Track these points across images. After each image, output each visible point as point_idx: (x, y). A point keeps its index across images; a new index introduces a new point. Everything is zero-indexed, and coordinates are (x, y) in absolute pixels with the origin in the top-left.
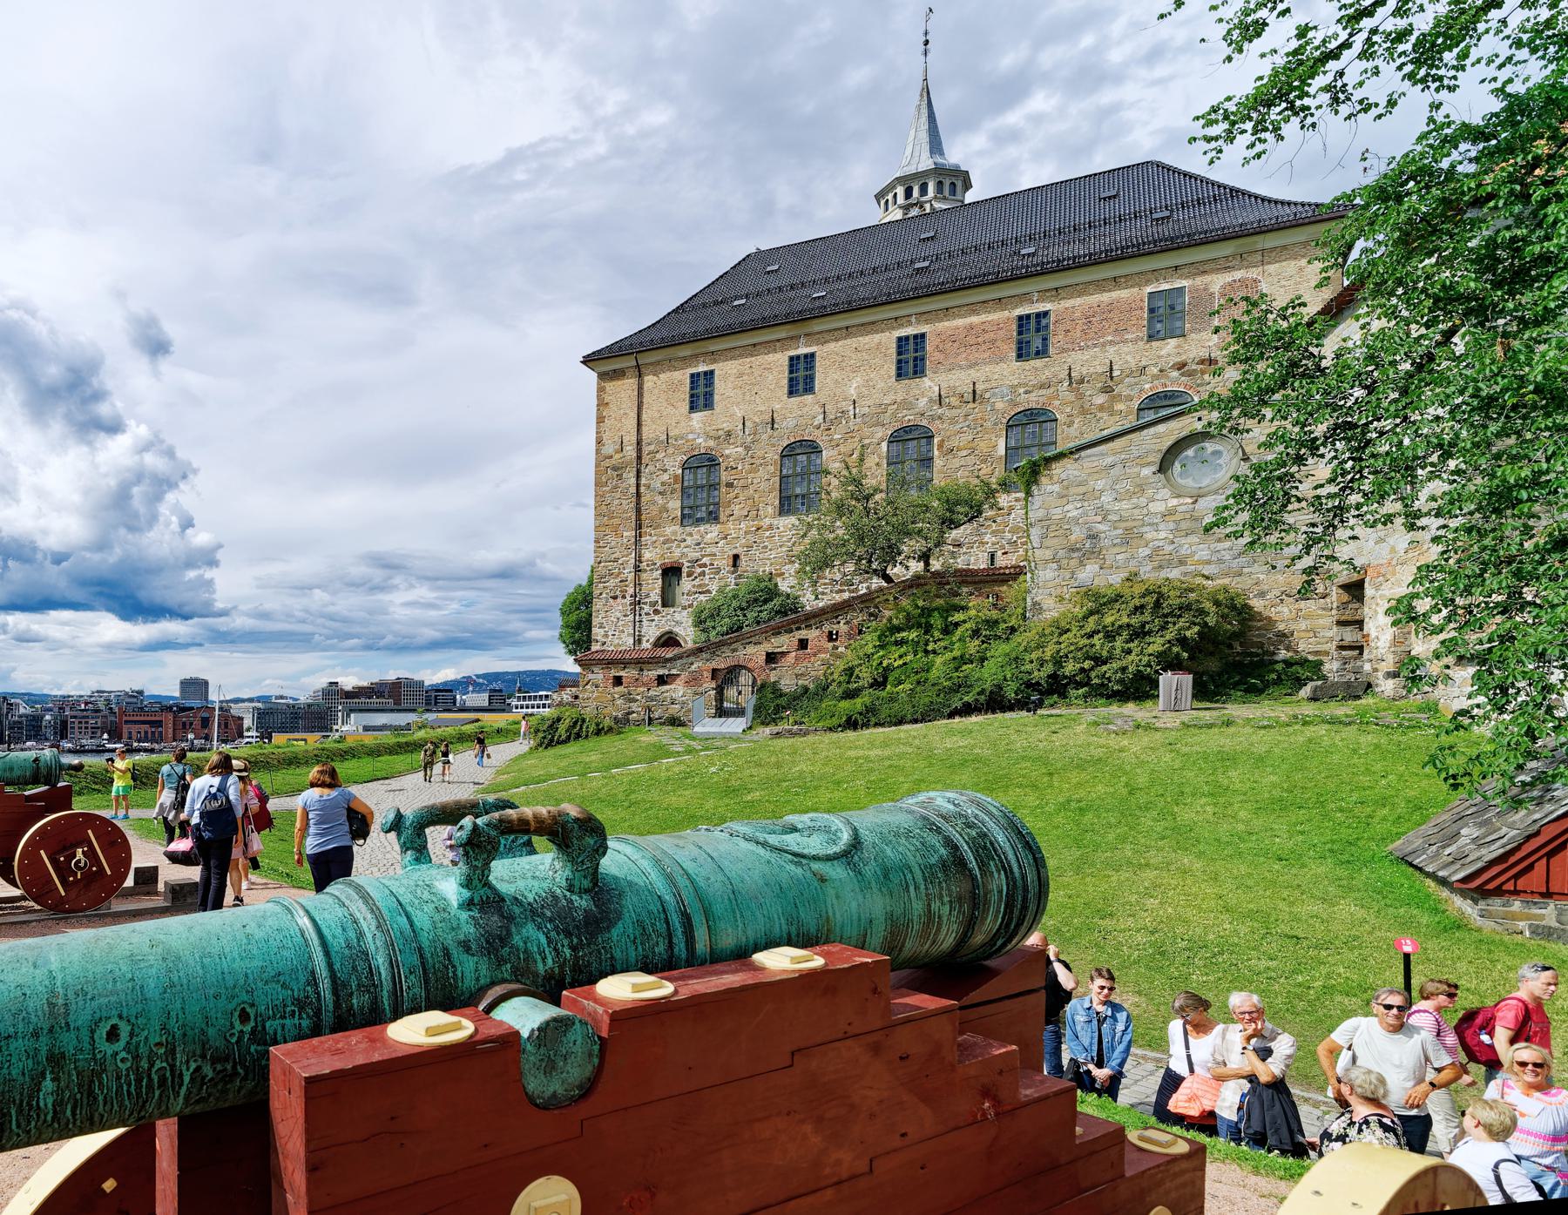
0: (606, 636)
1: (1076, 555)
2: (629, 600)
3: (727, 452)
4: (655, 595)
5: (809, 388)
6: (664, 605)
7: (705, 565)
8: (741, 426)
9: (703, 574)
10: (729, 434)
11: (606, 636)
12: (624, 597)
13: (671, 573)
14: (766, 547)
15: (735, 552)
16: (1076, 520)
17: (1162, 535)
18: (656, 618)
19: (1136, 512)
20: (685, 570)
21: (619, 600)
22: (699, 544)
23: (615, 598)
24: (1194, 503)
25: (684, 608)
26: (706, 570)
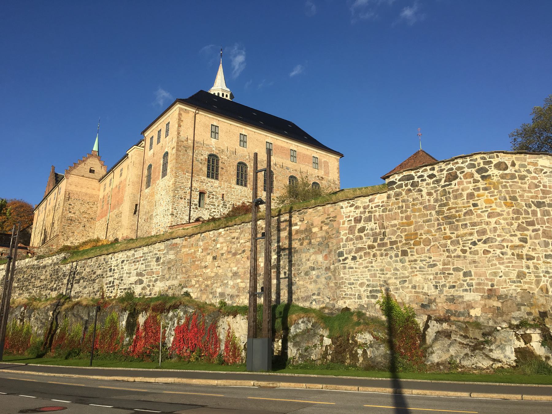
0: (177, 214)
4: (196, 201)
6: (199, 206)
7: (213, 195)
8: (226, 149)
9: (213, 198)
11: (177, 214)
12: (185, 199)
13: (202, 194)
14: (232, 194)
18: (196, 211)
21: (183, 199)
22: (212, 186)
23: (181, 198)
25: (206, 209)
26: (214, 197)
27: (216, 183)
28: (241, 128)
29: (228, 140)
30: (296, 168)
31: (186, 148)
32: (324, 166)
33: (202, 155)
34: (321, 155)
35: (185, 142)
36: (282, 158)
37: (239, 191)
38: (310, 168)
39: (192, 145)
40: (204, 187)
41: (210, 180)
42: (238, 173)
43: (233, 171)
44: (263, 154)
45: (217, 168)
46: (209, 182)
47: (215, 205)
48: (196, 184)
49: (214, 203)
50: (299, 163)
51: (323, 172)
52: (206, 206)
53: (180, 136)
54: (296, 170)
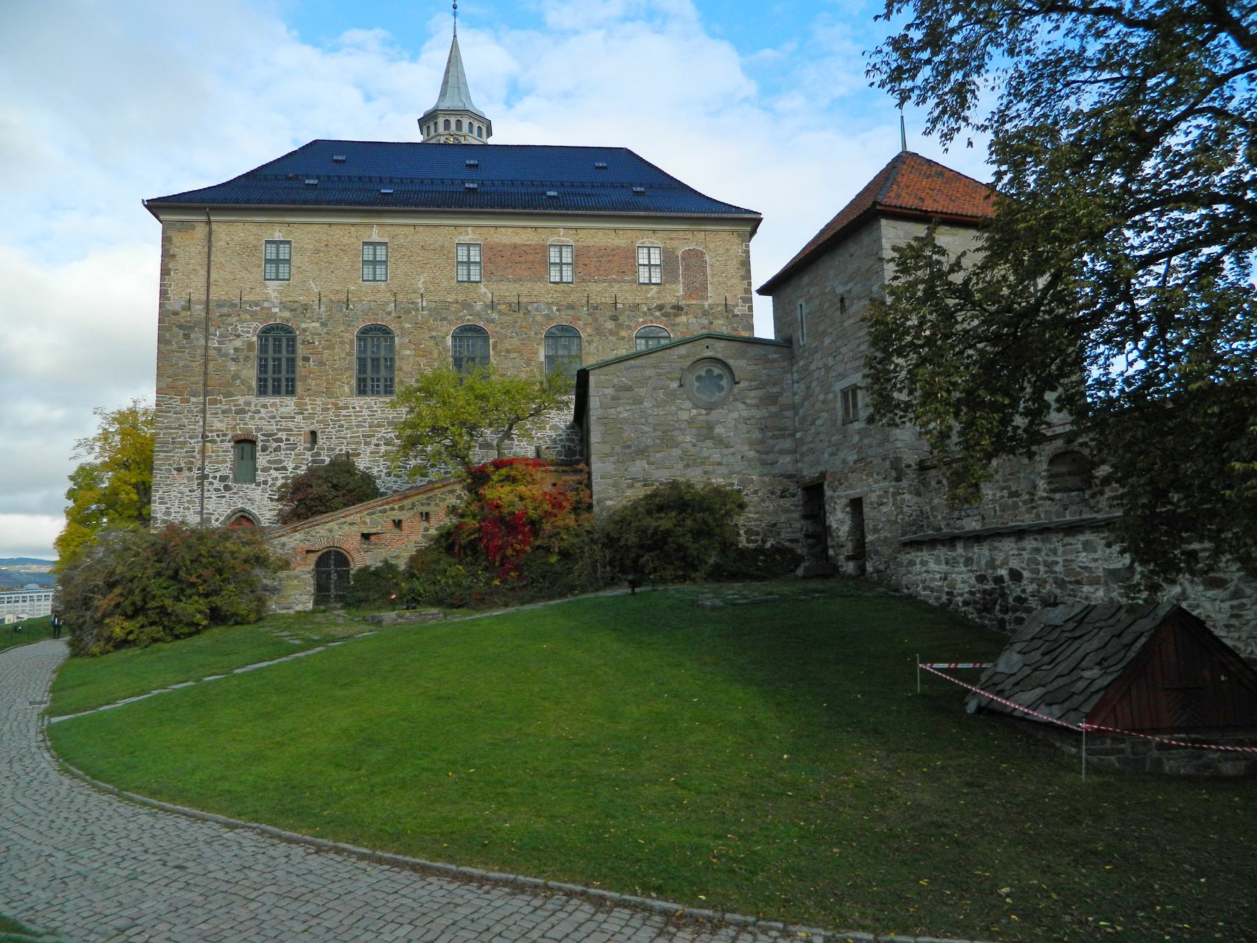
1: (627, 451)
2: (195, 473)
3: (304, 326)
7: (280, 440)
8: (317, 302)
9: (277, 449)
10: (305, 307)
12: (190, 469)
13: (245, 444)
14: (342, 426)
15: (312, 428)
16: (626, 420)
17: (688, 439)
19: (670, 418)
20: (260, 444)
21: (186, 473)
22: (274, 417)
23: (179, 470)
24: (707, 414)
27: (288, 404)
28: (365, 225)
29: (324, 274)
30: (573, 298)
31: (187, 329)
32: (687, 268)
33: (238, 336)
34: (673, 235)
35: (183, 314)
36: (519, 280)
37: (366, 412)
38: (625, 287)
39: (203, 314)
40: (251, 426)
41: (263, 400)
43: (343, 356)
44: (445, 284)
45: (292, 362)
46: (265, 406)
47: (285, 468)
48: (221, 421)
49: (281, 461)
50: (583, 281)
51: (681, 288)
52: (260, 477)
53: (168, 299)
54: (571, 307)
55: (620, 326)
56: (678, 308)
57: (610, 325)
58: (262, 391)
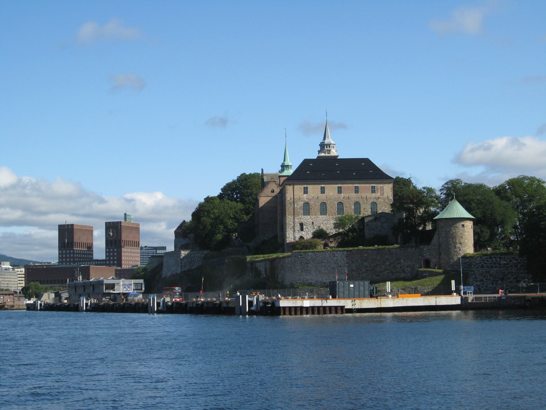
5: (324, 193)
10: (311, 199)
38: (369, 194)
40: (302, 221)
42: (321, 209)
54: (358, 198)
55: (368, 202)
56: (379, 198)
57: (366, 201)
58: (304, 215)
